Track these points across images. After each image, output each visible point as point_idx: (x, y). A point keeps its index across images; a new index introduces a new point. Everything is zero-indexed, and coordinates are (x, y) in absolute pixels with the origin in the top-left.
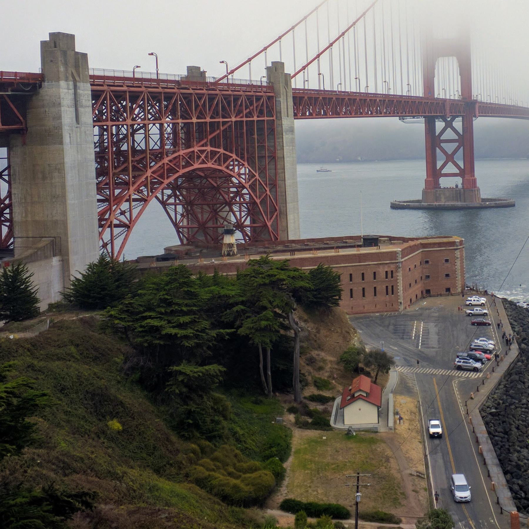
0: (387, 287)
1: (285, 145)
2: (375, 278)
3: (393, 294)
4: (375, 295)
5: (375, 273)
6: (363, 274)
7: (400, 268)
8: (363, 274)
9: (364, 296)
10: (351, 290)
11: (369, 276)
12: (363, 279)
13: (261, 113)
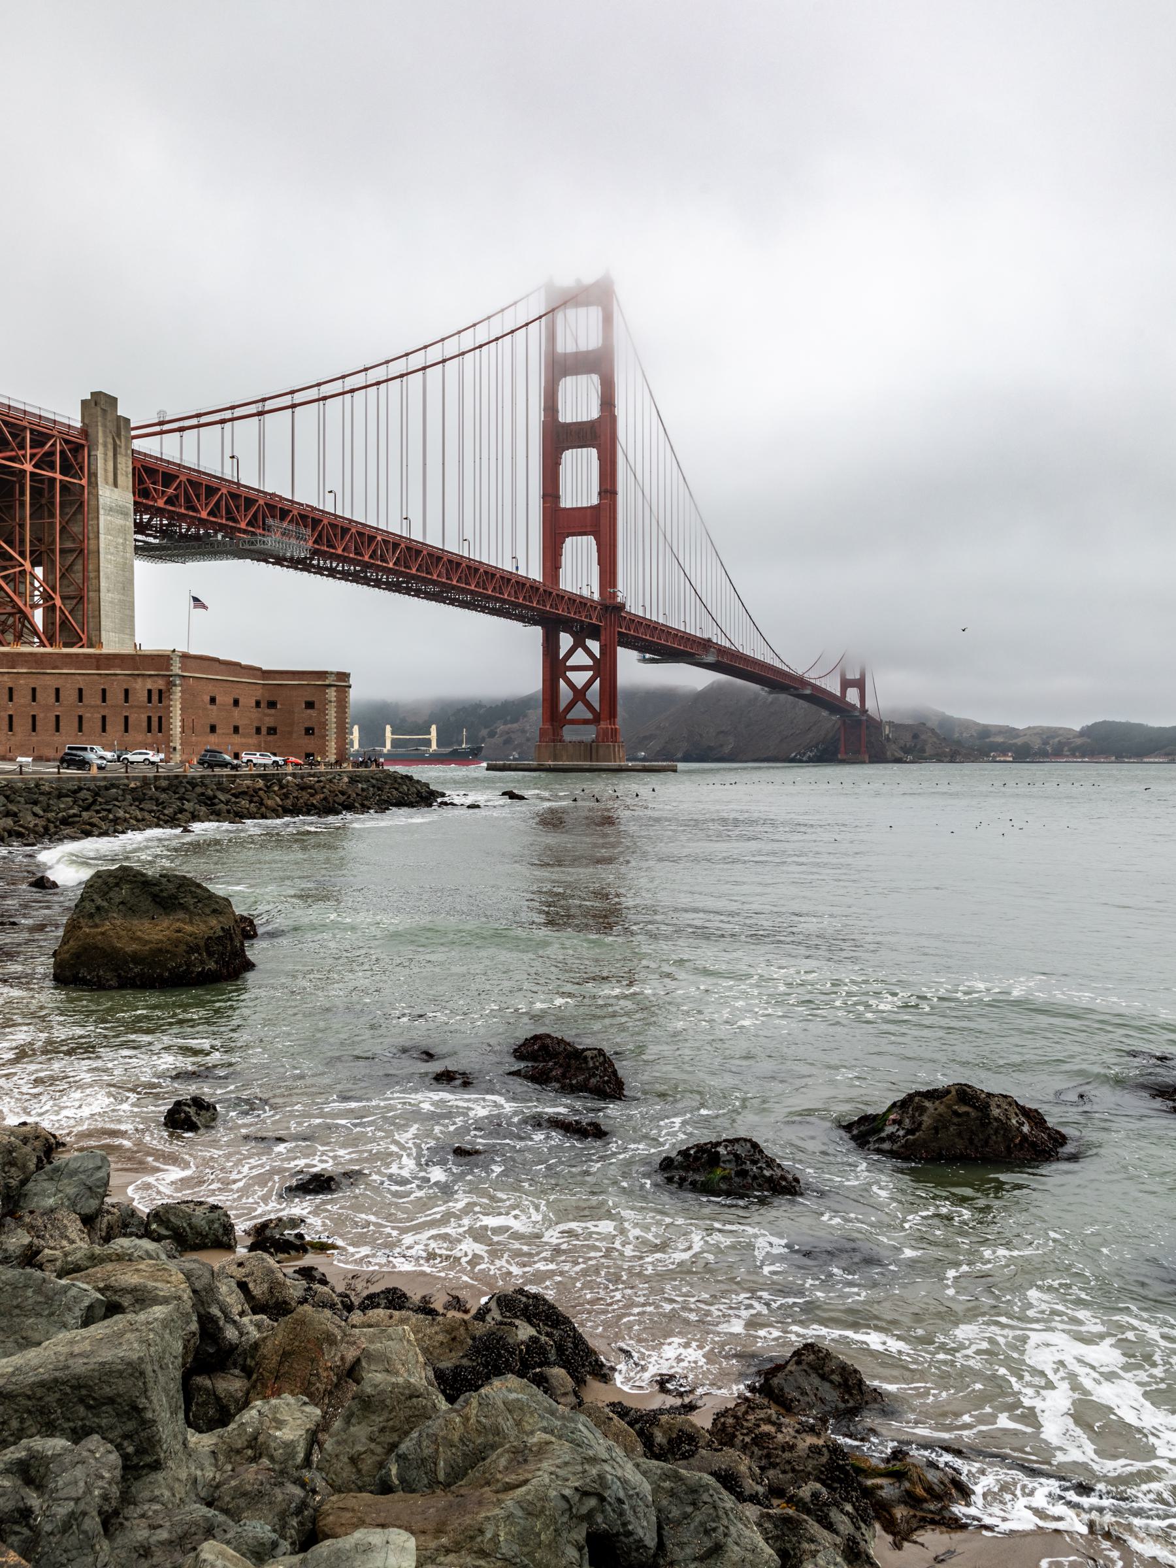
0: (149, 718)
1: (102, 531)
2: (126, 700)
3: (160, 731)
4: (126, 730)
5: (127, 691)
6: (104, 691)
7: (175, 685)
8: (104, 691)
9: (104, 730)
10: (80, 718)
11: (116, 696)
12: (104, 700)
13: (45, 462)
